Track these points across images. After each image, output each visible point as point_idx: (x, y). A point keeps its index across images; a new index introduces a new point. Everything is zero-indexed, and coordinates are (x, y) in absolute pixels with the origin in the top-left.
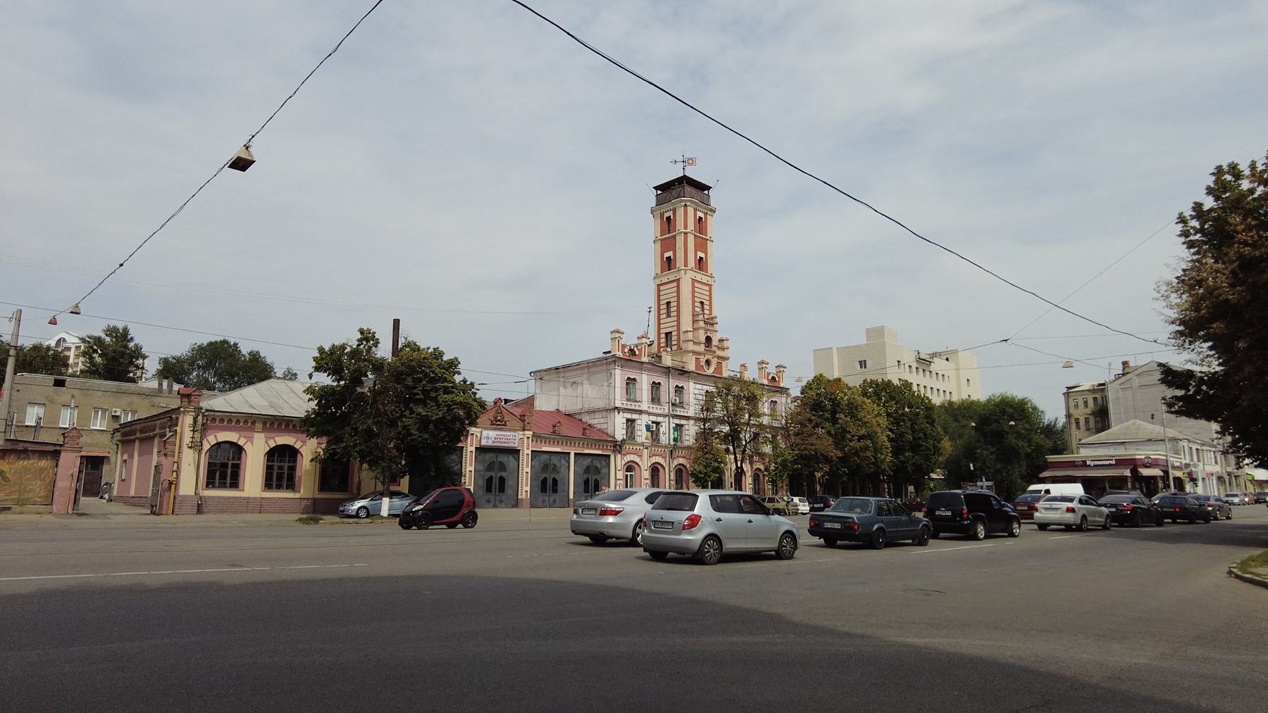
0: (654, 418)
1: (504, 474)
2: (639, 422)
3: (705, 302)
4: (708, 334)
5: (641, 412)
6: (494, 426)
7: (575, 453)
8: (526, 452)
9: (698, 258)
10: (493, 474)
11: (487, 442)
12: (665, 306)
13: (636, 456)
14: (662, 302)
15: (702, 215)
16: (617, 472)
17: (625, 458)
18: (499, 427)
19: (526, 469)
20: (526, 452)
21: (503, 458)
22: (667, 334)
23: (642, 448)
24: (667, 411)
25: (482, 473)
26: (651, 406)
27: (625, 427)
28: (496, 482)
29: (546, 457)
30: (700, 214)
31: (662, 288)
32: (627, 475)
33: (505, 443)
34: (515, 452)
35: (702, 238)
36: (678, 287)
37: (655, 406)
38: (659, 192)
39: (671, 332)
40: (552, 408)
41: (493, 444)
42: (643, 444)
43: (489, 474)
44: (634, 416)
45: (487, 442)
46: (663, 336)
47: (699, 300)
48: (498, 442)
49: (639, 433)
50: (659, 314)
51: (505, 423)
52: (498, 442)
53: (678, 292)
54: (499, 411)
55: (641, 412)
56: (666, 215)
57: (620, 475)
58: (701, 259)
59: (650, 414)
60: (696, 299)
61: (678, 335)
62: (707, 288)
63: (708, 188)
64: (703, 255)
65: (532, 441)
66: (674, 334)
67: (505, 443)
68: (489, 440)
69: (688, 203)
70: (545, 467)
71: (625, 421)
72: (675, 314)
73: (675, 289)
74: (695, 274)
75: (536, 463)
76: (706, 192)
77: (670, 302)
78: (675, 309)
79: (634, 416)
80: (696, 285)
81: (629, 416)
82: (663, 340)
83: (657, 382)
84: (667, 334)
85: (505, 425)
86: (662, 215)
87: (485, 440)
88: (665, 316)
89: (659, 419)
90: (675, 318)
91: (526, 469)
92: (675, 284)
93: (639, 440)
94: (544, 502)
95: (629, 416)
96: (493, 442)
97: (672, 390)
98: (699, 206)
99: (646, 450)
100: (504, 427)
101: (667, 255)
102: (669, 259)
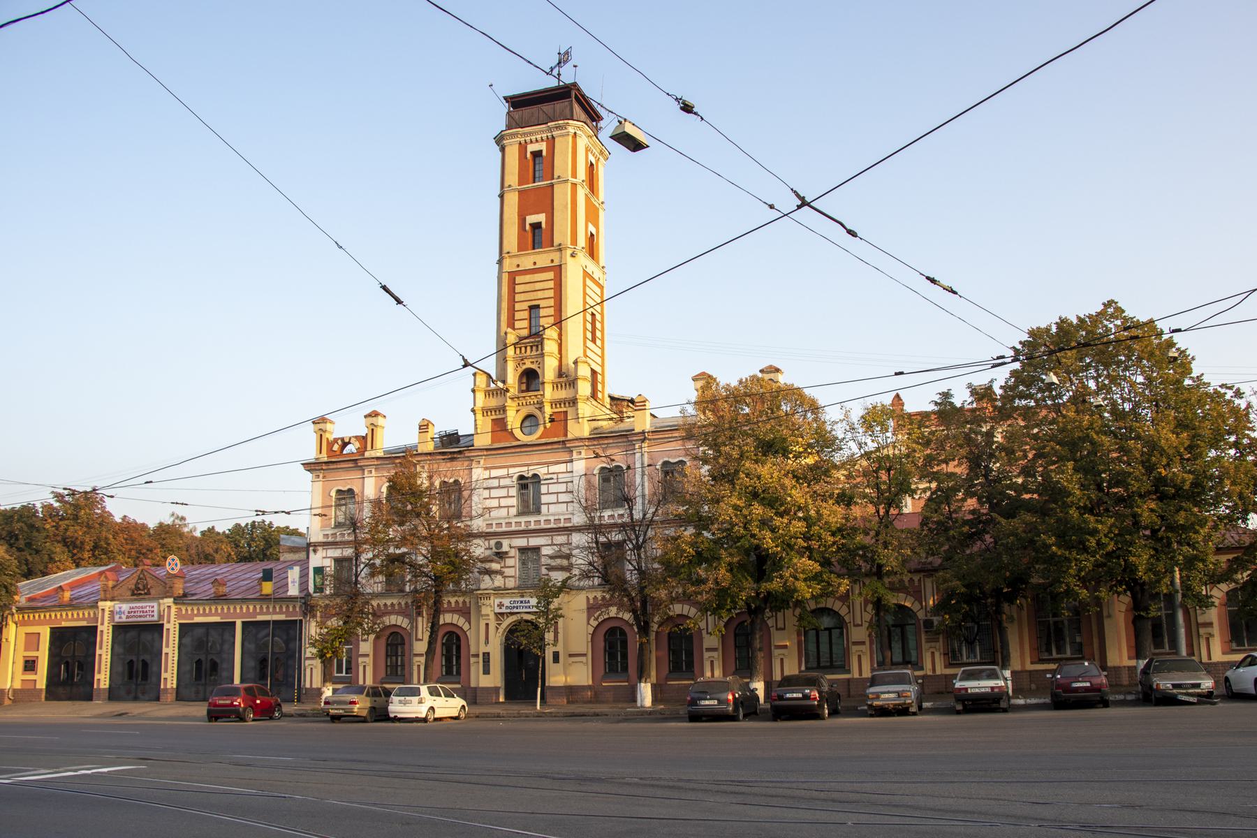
1: (147, 657)
3: (542, 303)
4: (528, 365)
6: (135, 597)
7: (243, 622)
10: (134, 658)
11: (120, 618)
15: (543, 147)
18: (141, 597)
19: (171, 650)
21: (147, 637)
25: (122, 657)
28: (139, 666)
29: (200, 631)
30: (531, 148)
33: (140, 616)
34: (156, 629)
41: (128, 620)
43: (129, 658)
45: (120, 618)
47: (525, 306)
48: (132, 617)
51: (149, 590)
52: (132, 617)
54: (142, 576)
58: (536, 226)
60: (517, 306)
62: (551, 275)
64: (541, 218)
67: (140, 616)
68: (123, 616)
70: (201, 645)
75: (187, 640)
80: (519, 279)
85: (148, 593)
87: (118, 616)
91: (171, 650)
94: (197, 692)
96: (128, 617)
100: (146, 597)
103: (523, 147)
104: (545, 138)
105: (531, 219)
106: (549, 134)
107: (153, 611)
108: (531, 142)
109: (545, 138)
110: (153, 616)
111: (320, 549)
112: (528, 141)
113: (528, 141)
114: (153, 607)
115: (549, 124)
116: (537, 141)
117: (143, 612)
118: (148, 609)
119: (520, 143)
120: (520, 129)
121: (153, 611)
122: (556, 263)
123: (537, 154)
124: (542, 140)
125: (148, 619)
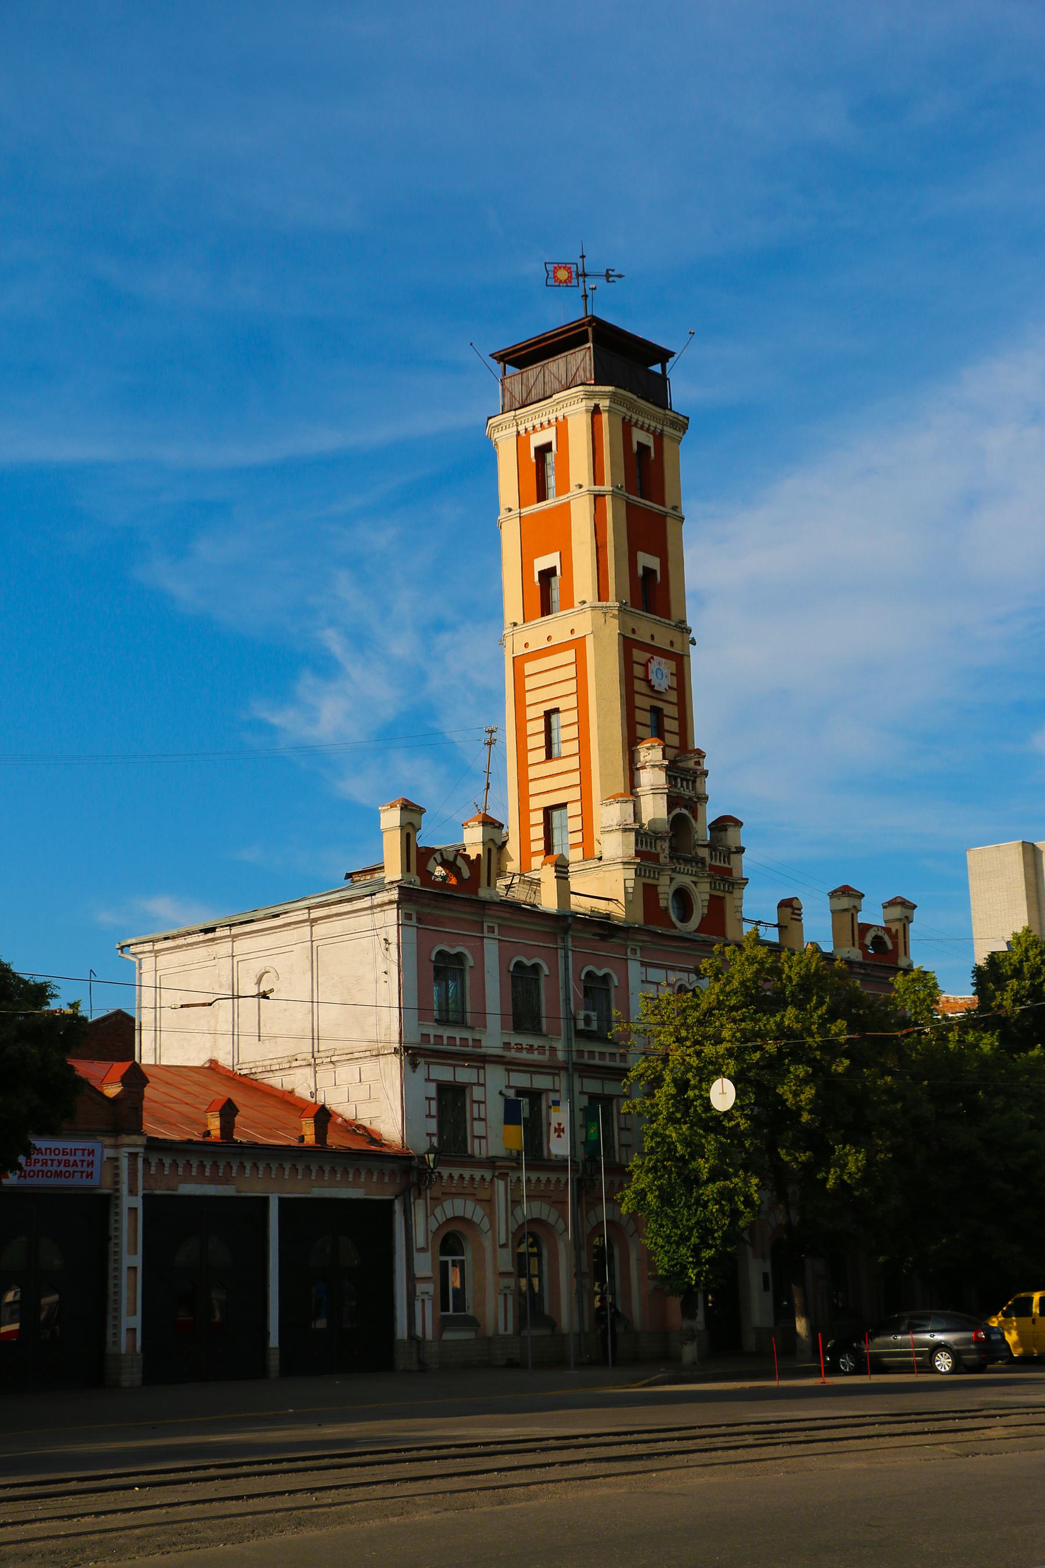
0: (521, 1080)
2: (477, 1093)
3: (671, 710)
5: (482, 1060)
8: (131, 1202)
9: (640, 572)
12: (540, 725)
13: (470, 1204)
14: (531, 713)
15: (648, 440)
16: (416, 1255)
17: (438, 1211)
20: (131, 1202)
22: (548, 811)
23: (488, 1175)
24: (561, 1056)
26: (515, 1039)
27: (434, 1112)
30: (639, 436)
31: (530, 667)
32: (444, 1265)
33: (58, 1174)
35: (649, 512)
36: (580, 663)
37: (525, 1040)
38: (511, 370)
39: (563, 806)
40: (198, 1059)
42: (490, 1163)
44: (464, 1075)
46: (537, 817)
49: (479, 1128)
50: (522, 751)
53: (581, 677)
55: (482, 1060)
56: (537, 440)
57: (424, 1265)
59: (511, 1065)
60: (639, 701)
61: (586, 816)
63: (664, 356)
64: (653, 562)
65: (146, 1161)
66: (574, 809)
67: (58, 1174)
69: (604, 404)
71: (432, 1090)
72: (573, 747)
73: (571, 672)
74: (631, 623)
76: (657, 368)
77: (556, 711)
78: (573, 732)
79: (464, 1075)
80: (638, 655)
81: (444, 1073)
82: (538, 832)
83: (528, 963)
84: (548, 811)
86: (522, 441)
88: (542, 754)
89: (541, 1082)
90: (574, 763)
92: (570, 656)
93: (477, 1149)
95: (444, 1073)
97: (576, 991)
98: (640, 411)
99: (500, 1185)
101: (542, 563)
102: (547, 575)
103: (627, 426)
104: (652, 428)
105: (647, 560)
106: (659, 427)
107: (91, 1164)
108: (636, 425)
109: (652, 428)
110: (90, 1175)
111: (421, 1061)
112: (634, 420)
113: (634, 420)
114: (92, 1152)
115: (668, 412)
116: (642, 428)
117: (67, 1163)
118: (78, 1157)
119: (624, 419)
120: (635, 397)
121: (91, 1164)
122: (677, 649)
123: (643, 448)
124: (648, 430)
125: (78, 1181)
